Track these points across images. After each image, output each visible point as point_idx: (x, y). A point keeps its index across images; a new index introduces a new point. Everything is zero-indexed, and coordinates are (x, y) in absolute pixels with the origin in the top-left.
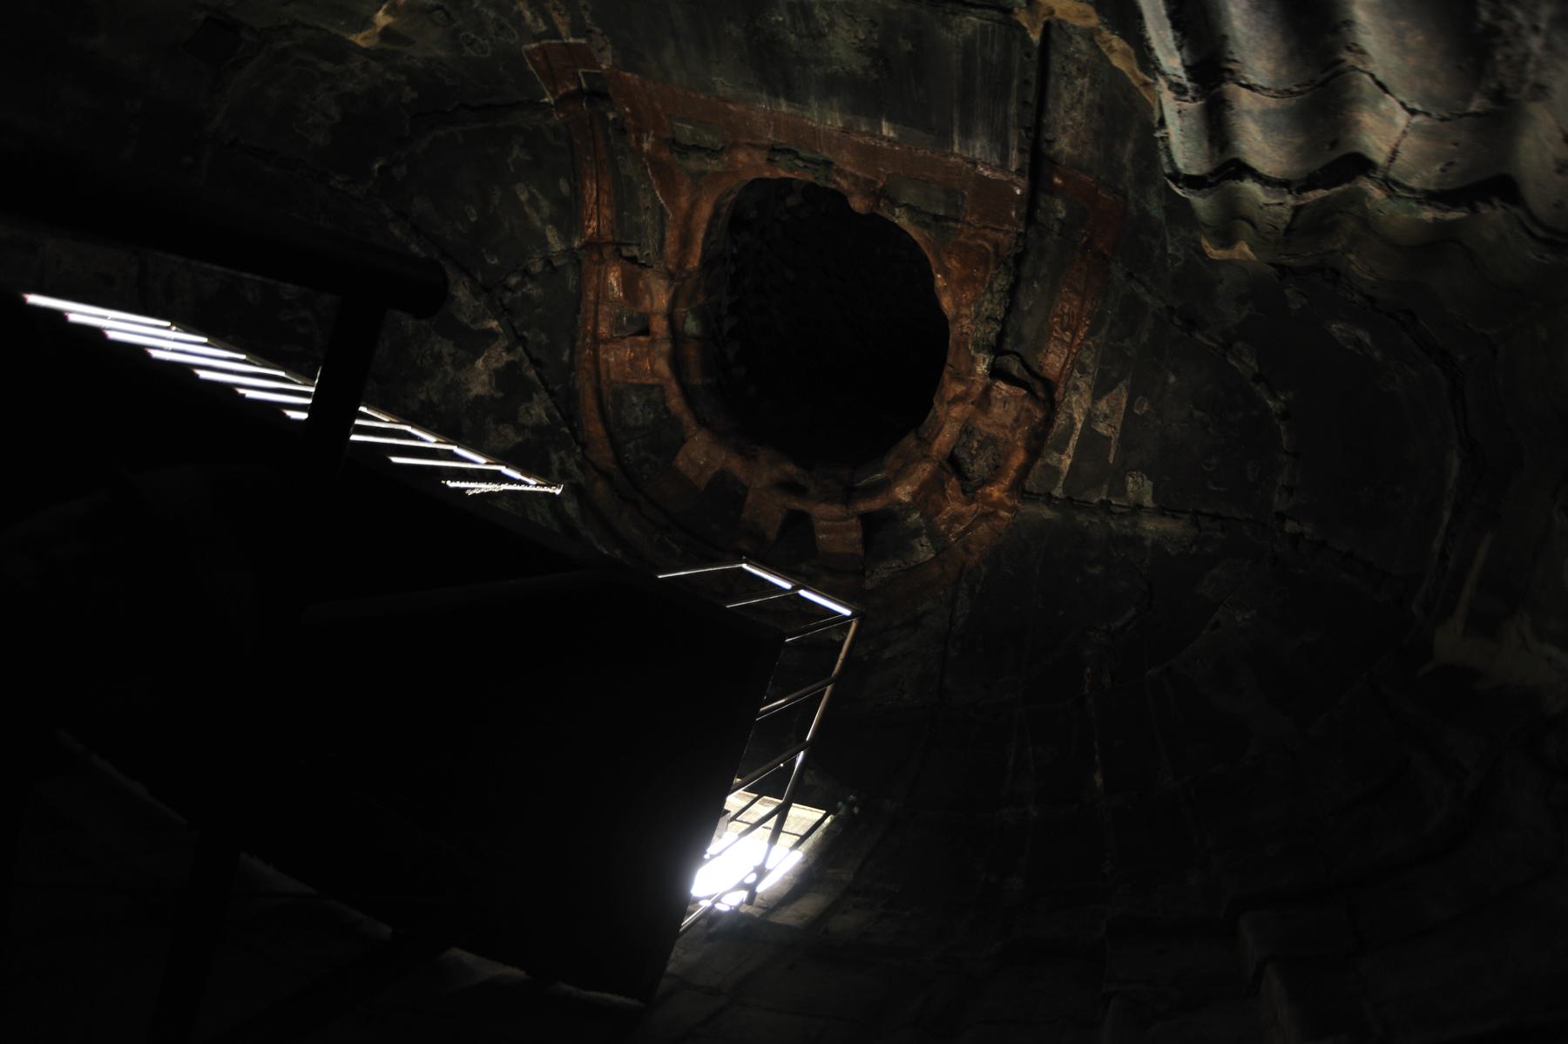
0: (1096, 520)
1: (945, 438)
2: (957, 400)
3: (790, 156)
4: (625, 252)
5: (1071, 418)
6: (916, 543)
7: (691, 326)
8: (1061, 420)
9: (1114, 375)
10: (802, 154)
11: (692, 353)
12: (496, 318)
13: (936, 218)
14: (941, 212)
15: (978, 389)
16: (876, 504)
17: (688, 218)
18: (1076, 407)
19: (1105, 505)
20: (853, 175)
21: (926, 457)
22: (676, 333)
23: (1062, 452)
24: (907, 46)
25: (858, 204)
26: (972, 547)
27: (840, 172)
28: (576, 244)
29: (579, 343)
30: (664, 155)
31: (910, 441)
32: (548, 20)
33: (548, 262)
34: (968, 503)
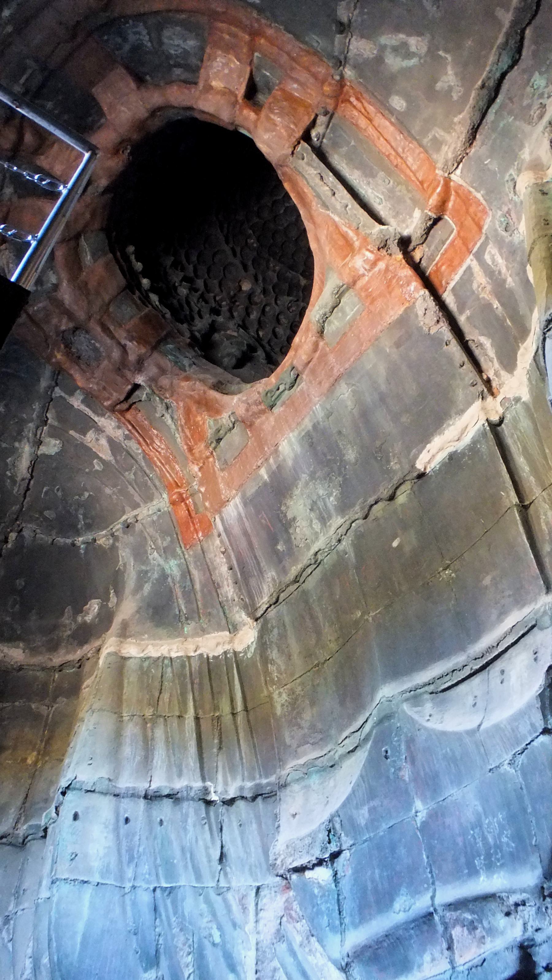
0: (34, 416)
3: (287, 387)
4: (322, 119)
5: (103, 415)
9: (118, 458)
13: (219, 440)
14: (222, 443)
19: (45, 422)
23: (83, 402)
28: (349, 73)
29: (255, 14)
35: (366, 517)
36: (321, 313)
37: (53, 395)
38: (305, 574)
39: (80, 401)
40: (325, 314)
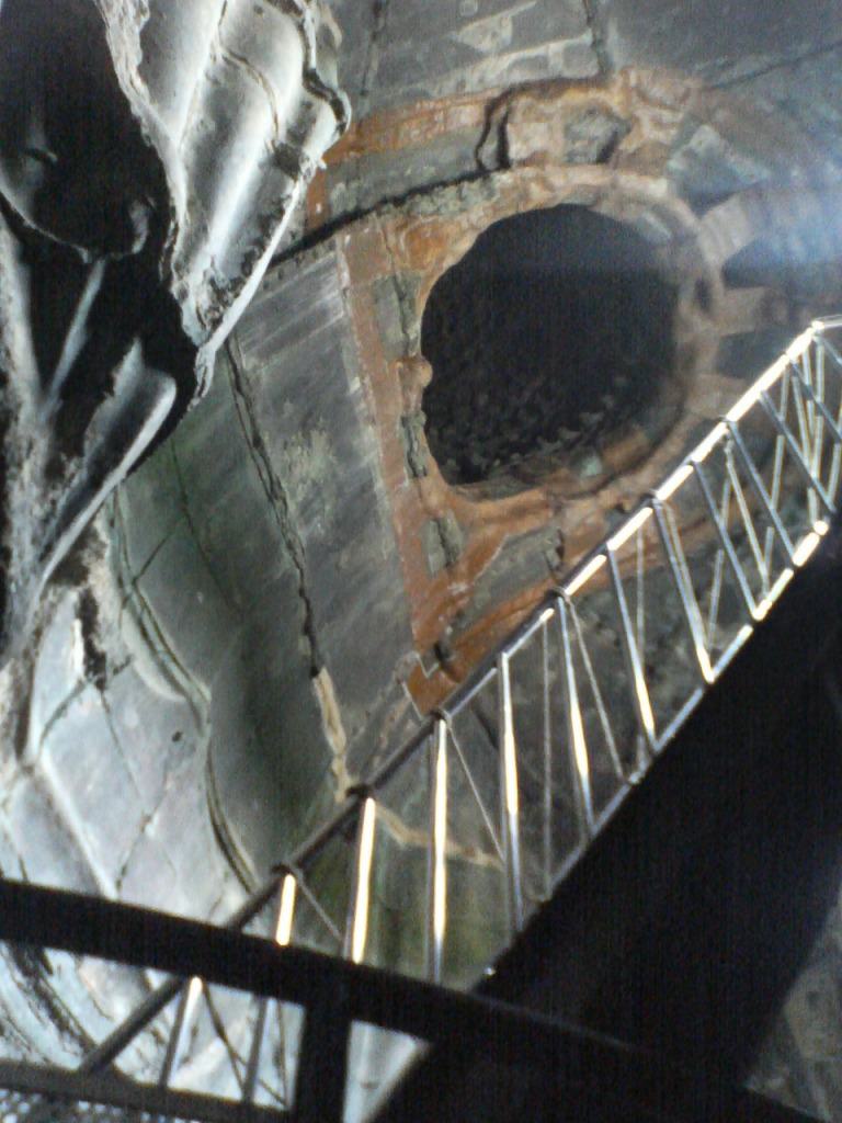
1: (588, 177)
2: (545, 183)
4: (556, 561)
6: (701, 150)
7: (592, 468)
8: (518, 77)
10: (406, 447)
11: (618, 455)
12: (672, 650)
13: (401, 299)
14: (394, 296)
15: (529, 172)
16: (682, 210)
17: (501, 520)
18: (498, 70)
20: (403, 394)
21: (614, 186)
22: (608, 479)
24: (288, 407)
25: (425, 375)
26: (681, 90)
27: (407, 406)
30: (463, 568)
31: (605, 209)
32: (404, 722)
33: (599, 626)
34: (637, 120)
35: (301, 592)
36: (450, 528)
37: (590, 30)
38: (260, 461)
39: (550, 54)
40: (445, 529)
